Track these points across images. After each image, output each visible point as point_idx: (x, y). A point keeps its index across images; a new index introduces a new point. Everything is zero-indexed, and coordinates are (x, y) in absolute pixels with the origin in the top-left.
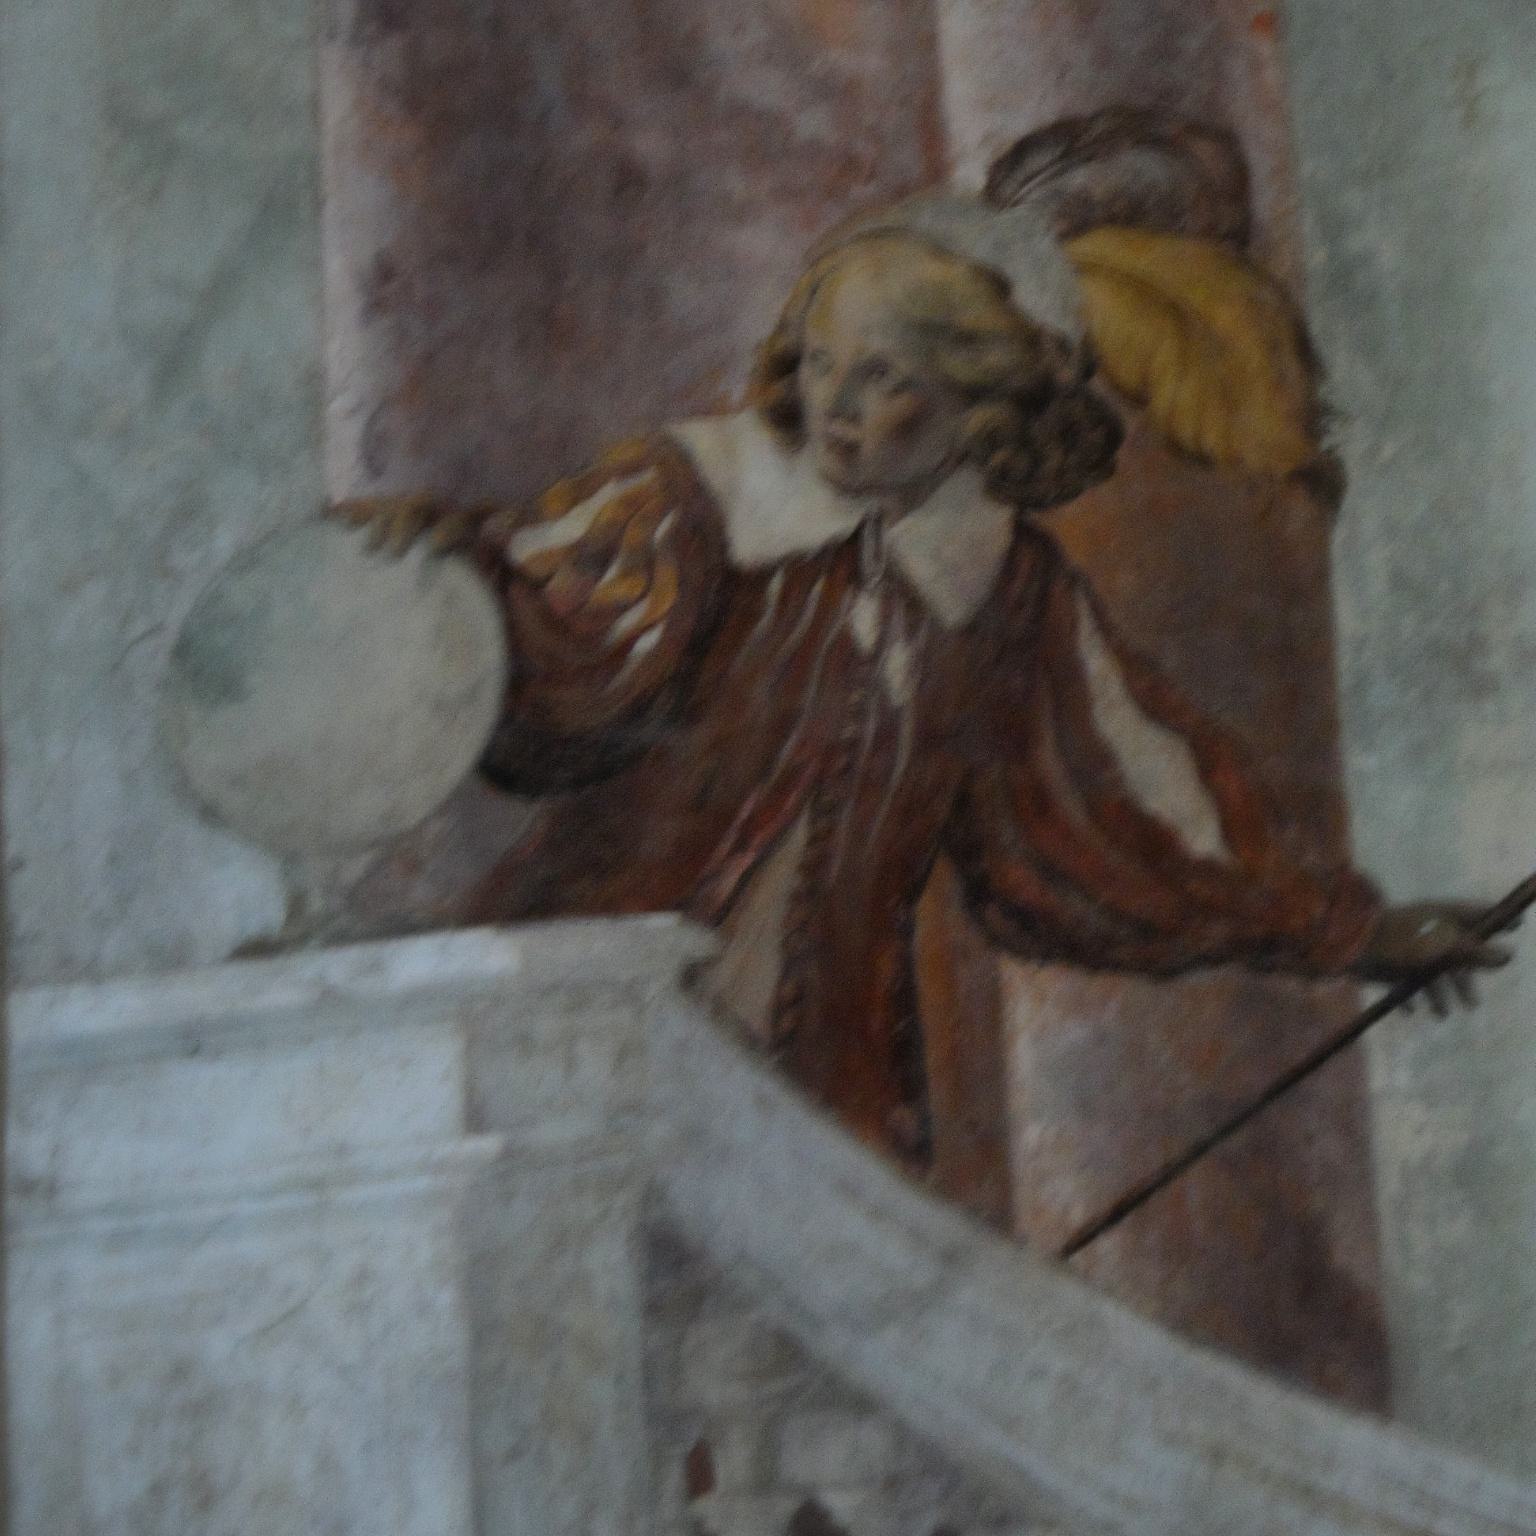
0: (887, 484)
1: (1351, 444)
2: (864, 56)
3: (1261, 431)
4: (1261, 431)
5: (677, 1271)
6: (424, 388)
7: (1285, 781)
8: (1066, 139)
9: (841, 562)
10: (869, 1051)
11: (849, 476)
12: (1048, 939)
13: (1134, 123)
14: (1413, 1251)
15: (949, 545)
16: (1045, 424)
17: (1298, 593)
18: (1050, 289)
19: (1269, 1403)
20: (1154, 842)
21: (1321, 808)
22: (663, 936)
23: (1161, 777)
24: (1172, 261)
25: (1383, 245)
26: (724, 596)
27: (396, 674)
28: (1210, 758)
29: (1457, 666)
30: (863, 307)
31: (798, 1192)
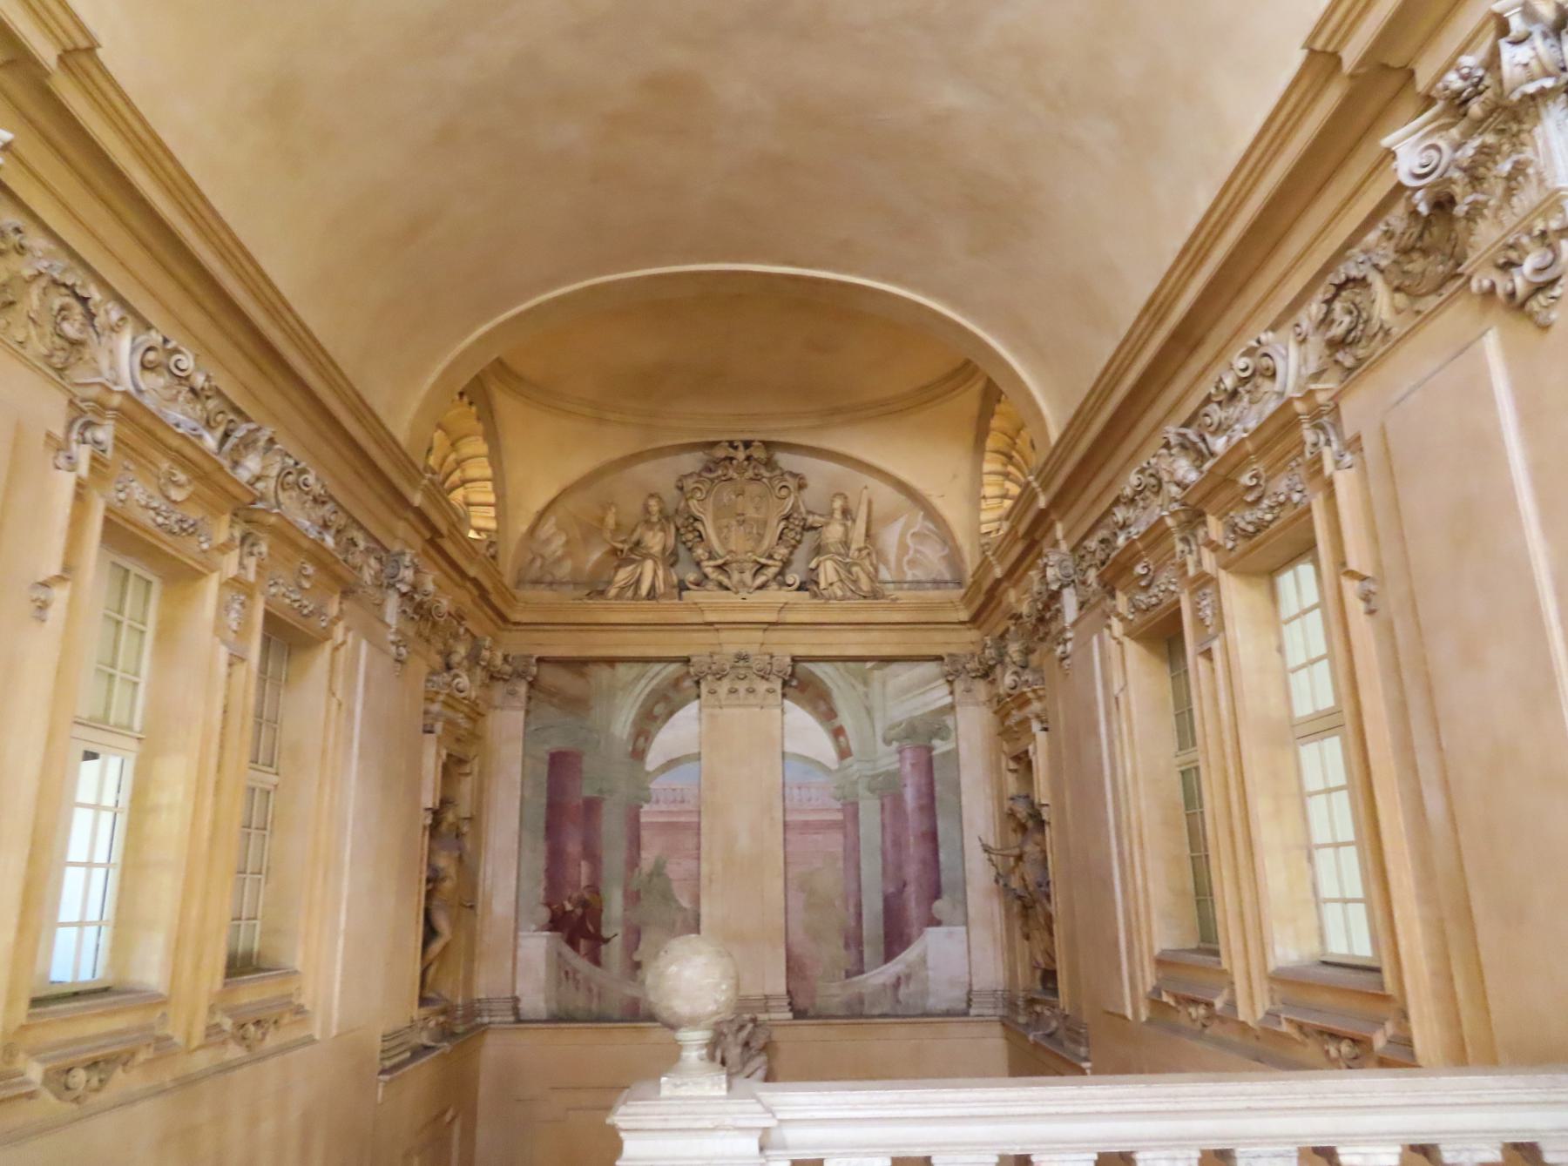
0: (575, 906)
5: (560, 955)
6: (547, 897)
7: (598, 927)
10: (572, 942)
12: (585, 937)
14: (603, 959)
15: (579, 911)
16: (584, 904)
18: (587, 896)
19: (593, 967)
22: (558, 934)
23: (590, 928)
26: (565, 912)
27: (544, 914)
30: (575, 895)
31: (567, 950)
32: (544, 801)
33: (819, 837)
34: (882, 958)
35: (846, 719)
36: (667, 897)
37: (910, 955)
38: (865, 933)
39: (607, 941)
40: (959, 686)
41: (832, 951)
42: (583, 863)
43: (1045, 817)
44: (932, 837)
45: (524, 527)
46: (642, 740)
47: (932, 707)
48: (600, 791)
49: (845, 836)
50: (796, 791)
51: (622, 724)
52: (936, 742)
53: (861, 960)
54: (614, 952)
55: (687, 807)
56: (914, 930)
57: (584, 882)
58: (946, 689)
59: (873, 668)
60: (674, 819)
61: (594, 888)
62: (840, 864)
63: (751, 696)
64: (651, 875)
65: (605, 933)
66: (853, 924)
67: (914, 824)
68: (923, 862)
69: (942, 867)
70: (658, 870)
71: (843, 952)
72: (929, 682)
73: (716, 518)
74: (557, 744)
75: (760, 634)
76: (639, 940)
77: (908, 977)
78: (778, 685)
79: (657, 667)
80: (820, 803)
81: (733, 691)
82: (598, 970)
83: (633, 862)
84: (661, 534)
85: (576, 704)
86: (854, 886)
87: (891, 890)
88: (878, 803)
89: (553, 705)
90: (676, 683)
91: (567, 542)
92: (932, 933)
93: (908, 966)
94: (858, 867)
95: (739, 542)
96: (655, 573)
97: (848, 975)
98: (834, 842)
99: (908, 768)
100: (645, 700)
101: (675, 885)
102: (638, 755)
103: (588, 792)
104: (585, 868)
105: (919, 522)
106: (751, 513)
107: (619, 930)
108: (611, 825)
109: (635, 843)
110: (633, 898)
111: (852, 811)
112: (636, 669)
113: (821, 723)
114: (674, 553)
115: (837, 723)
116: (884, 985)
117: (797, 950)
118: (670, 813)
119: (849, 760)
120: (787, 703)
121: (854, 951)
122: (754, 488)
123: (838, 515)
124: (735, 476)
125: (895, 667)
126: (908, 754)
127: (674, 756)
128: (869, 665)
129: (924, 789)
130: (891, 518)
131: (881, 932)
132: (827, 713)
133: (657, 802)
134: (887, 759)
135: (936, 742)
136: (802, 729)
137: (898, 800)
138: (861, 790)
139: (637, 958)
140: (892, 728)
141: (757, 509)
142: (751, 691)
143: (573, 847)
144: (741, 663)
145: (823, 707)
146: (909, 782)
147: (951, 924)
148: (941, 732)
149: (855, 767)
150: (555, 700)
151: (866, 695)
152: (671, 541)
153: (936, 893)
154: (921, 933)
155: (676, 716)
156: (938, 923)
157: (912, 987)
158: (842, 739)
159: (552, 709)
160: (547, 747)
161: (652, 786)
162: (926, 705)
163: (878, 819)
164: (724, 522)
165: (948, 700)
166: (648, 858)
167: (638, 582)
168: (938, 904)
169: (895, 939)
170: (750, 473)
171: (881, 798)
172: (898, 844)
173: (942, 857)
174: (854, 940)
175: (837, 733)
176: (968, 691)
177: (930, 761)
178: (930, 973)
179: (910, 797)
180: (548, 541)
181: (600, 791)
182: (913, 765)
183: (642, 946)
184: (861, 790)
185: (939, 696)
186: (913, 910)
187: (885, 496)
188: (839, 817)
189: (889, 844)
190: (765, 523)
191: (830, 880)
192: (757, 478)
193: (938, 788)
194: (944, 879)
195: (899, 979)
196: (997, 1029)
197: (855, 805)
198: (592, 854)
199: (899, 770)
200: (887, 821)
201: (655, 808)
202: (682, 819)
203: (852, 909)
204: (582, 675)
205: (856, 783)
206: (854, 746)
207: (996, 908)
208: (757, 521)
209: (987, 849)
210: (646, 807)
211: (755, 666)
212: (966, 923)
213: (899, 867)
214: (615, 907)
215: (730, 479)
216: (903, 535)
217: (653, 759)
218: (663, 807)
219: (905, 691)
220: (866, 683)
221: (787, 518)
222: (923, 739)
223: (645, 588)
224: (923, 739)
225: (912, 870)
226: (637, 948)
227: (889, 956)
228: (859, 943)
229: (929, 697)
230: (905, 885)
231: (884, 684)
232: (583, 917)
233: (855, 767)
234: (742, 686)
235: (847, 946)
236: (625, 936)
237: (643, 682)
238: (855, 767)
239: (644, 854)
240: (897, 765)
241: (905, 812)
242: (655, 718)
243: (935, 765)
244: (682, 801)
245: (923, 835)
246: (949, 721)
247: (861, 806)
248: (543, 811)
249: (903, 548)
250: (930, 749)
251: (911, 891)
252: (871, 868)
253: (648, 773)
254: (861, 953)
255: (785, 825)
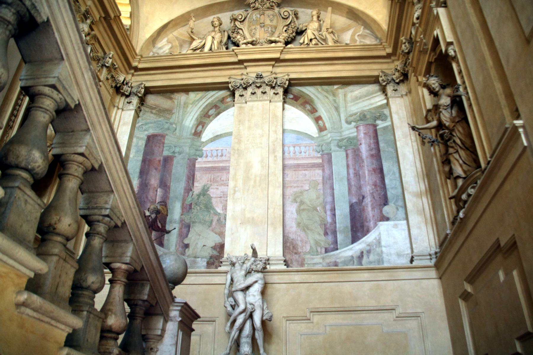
0: (152, 213)
1: (169, 214)
2: (154, 198)
3: (165, 213)
4: (165, 213)
7: (164, 225)
8: (161, 202)
9: (149, 216)
11: (150, 213)
13: (163, 202)
14: (165, 242)
15: (153, 216)
16: (158, 212)
17: (166, 219)
18: (159, 207)
20: (159, 227)
21: (165, 227)
23: (159, 225)
24: (164, 207)
25: (171, 207)
28: (161, 224)
29: (171, 222)
30: (152, 207)
32: (140, 158)
33: (306, 172)
34: (350, 240)
35: (322, 112)
36: (208, 207)
37: (370, 238)
38: (338, 225)
39: (168, 232)
40: (390, 89)
41: (317, 235)
42: (159, 190)
43: (451, 53)
44: (380, 171)
45: (148, 36)
46: (200, 127)
47: (375, 106)
48: (174, 152)
49: (323, 170)
50: (292, 149)
51: (190, 121)
52: (378, 122)
53: (336, 242)
54: (172, 239)
55: (224, 158)
56: (372, 224)
57: (158, 200)
58: (383, 97)
59: (338, 88)
60: (216, 165)
61: (164, 203)
62: (320, 186)
63: (265, 95)
64: (199, 196)
65: (168, 228)
66: (329, 220)
67: (368, 164)
68: (375, 185)
69: (387, 187)
70: (205, 192)
71: (323, 238)
72: (372, 94)
73: (249, 26)
74: (151, 132)
75: (270, 68)
76: (189, 231)
77: (369, 252)
78: (281, 91)
79: (212, 93)
80: (309, 154)
81: (253, 94)
82: (162, 249)
83: (189, 189)
84: (219, 34)
85: (165, 112)
86: (329, 199)
87: (354, 200)
88: (344, 154)
89: (152, 113)
90: (222, 100)
91: (171, 48)
92: (383, 226)
93: (369, 245)
94: (332, 189)
95: (261, 35)
96: (213, 42)
97: (327, 251)
98: (317, 174)
99: (362, 135)
100: (204, 108)
101: (214, 201)
102: (197, 134)
103: (166, 153)
104: (160, 192)
105: (361, 30)
106: (268, 22)
107: (177, 226)
108: (179, 169)
109: (191, 178)
110: (187, 208)
111: (328, 158)
112: (200, 94)
113: (308, 115)
114: (226, 44)
115: (317, 115)
116: (352, 257)
117: (292, 236)
118: (215, 162)
119: (324, 133)
120: (286, 106)
121: (330, 238)
122: (270, 12)
123: (315, 18)
124: (260, 6)
125: (351, 88)
126: (361, 128)
127: (219, 134)
128: (336, 87)
129: (373, 146)
130: (344, 30)
131: (349, 225)
132: (312, 111)
133: (207, 156)
134: (349, 131)
135: (378, 122)
136: (297, 119)
137: (357, 153)
138: (333, 147)
139: (186, 242)
140: (351, 116)
141: (271, 21)
142: (264, 93)
143: (154, 181)
144: (258, 81)
145: (308, 107)
146: (363, 141)
147: (396, 219)
148: (382, 117)
149: (328, 136)
150: (154, 111)
151: (335, 101)
152: (225, 39)
153: (385, 201)
154: (376, 225)
155: (221, 115)
156: (388, 219)
157: (372, 257)
158: (320, 122)
159: (152, 115)
160: (146, 133)
161: (204, 149)
162: (371, 104)
163: (345, 162)
164: (253, 27)
165: (385, 101)
166: (198, 187)
167: (203, 46)
168: (386, 210)
169: (358, 228)
170: (268, 5)
171: (346, 151)
172: (357, 175)
173: (387, 181)
174: (330, 230)
175: (318, 119)
176: (396, 90)
177: (376, 131)
178: (384, 249)
179: (364, 150)
180: (160, 48)
181: (174, 152)
182: (365, 134)
183: (189, 236)
184: (333, 147)
185: (379, 100)
186: (370, 212)
187: (341, 20)
188: (320, 161)
189: (352, 175)
190: (276, 28)
191: (312, 196)
192: (271, 8)
193: (382, 145)
194: (389, 194)
195: (362, 253)
196: (433, 273)
197: (330, 155)
198: (164, 185)
199: (357, 136)
200: (350, 163)
201: (204, 159)
202: (221, 165)
203: (329, 213)
204: (171, 99)
205: (330, 143)
206: (328, 125)
207: (426, 202)
208: (271, 26)
209: (413, 128)
210: (199, 159)
211: (266, 80)
212: (407, 219)
213: (360, 188)
214: (176, 212)
215: (257, 9)
216: (353, 35)
217: (206, 135)
218: (209, 159)
219: (357, 98)
220: (334, 95)
221: (288, 25)
222: (373, 124)
223: (207, 49)
224: (373, 124)
225: (367, 189)
226: (187, 236)
227: (355, 239)
228: (334, 233)
229: (373, 101)
230: (363, 197)
231: (345, 95)
232: (155, 220)
233: (329, 135)
234: (259, 91)
235: (326, 234)
236: (181, 229)
237: (204, 100)
238: (329, 135)
239: (196, 184)
240: (355, 134)
241: (361, 158)
242: (209, 117)
243: (379, 133)
244: (222, 156)
245: (374, 170)
246: (386, 112)
247: (332, 155)
248: (139, 164)
249: (353, 39)
250: (375, 126)
251: (368, 201)
252: (341, 189)
253: (203, 142)
254: (336, 237)
255: (284, 167)
